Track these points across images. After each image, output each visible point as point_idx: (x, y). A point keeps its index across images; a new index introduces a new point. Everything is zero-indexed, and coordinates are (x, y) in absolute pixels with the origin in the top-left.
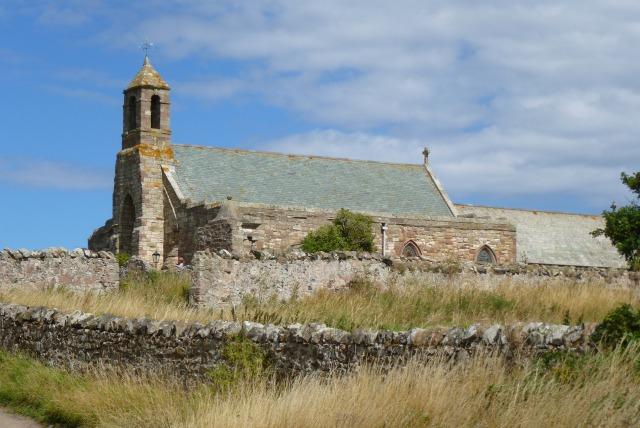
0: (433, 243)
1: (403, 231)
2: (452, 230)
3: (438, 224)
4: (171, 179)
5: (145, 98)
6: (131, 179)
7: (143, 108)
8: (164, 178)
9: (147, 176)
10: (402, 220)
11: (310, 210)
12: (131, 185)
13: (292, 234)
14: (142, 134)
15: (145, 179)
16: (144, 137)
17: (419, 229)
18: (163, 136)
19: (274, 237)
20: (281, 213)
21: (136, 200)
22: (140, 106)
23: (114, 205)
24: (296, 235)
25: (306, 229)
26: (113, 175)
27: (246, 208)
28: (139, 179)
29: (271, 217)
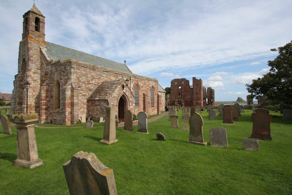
0: (142, 84)
1: (135, 80)
2: (146, 81)
3: (144, 78)
4: (44, 52)
5: (32, 17)
6: (25, 51)
7: (31, 21)
8: (41, 52)
9: (32, 50)
10: (135, 76)
11: (108, 69)
12: (24, 54)
13: (102, 78)
14: (30, 32)
15: (31, 51)
16: (31, 33)
17: (139, 80)
18: (41, 35)
19: (95, 79)
20: (98, 68)
21: (26, 60)
22: (29, 19)
23: (18, 63)
24: (104, 79)
25: (107, 76)
26: (18, 51)
27: (83, 64)
28: (28, 51)
29: (94, 70)
